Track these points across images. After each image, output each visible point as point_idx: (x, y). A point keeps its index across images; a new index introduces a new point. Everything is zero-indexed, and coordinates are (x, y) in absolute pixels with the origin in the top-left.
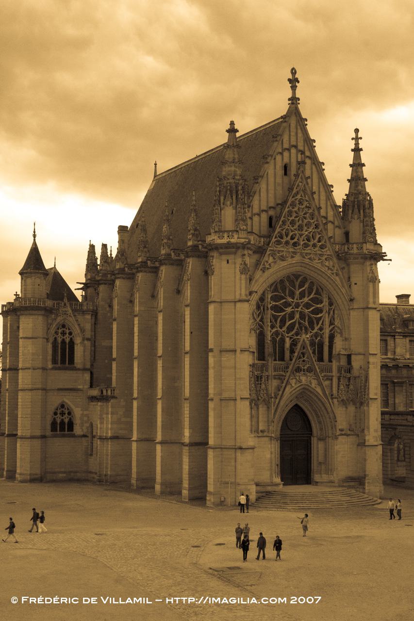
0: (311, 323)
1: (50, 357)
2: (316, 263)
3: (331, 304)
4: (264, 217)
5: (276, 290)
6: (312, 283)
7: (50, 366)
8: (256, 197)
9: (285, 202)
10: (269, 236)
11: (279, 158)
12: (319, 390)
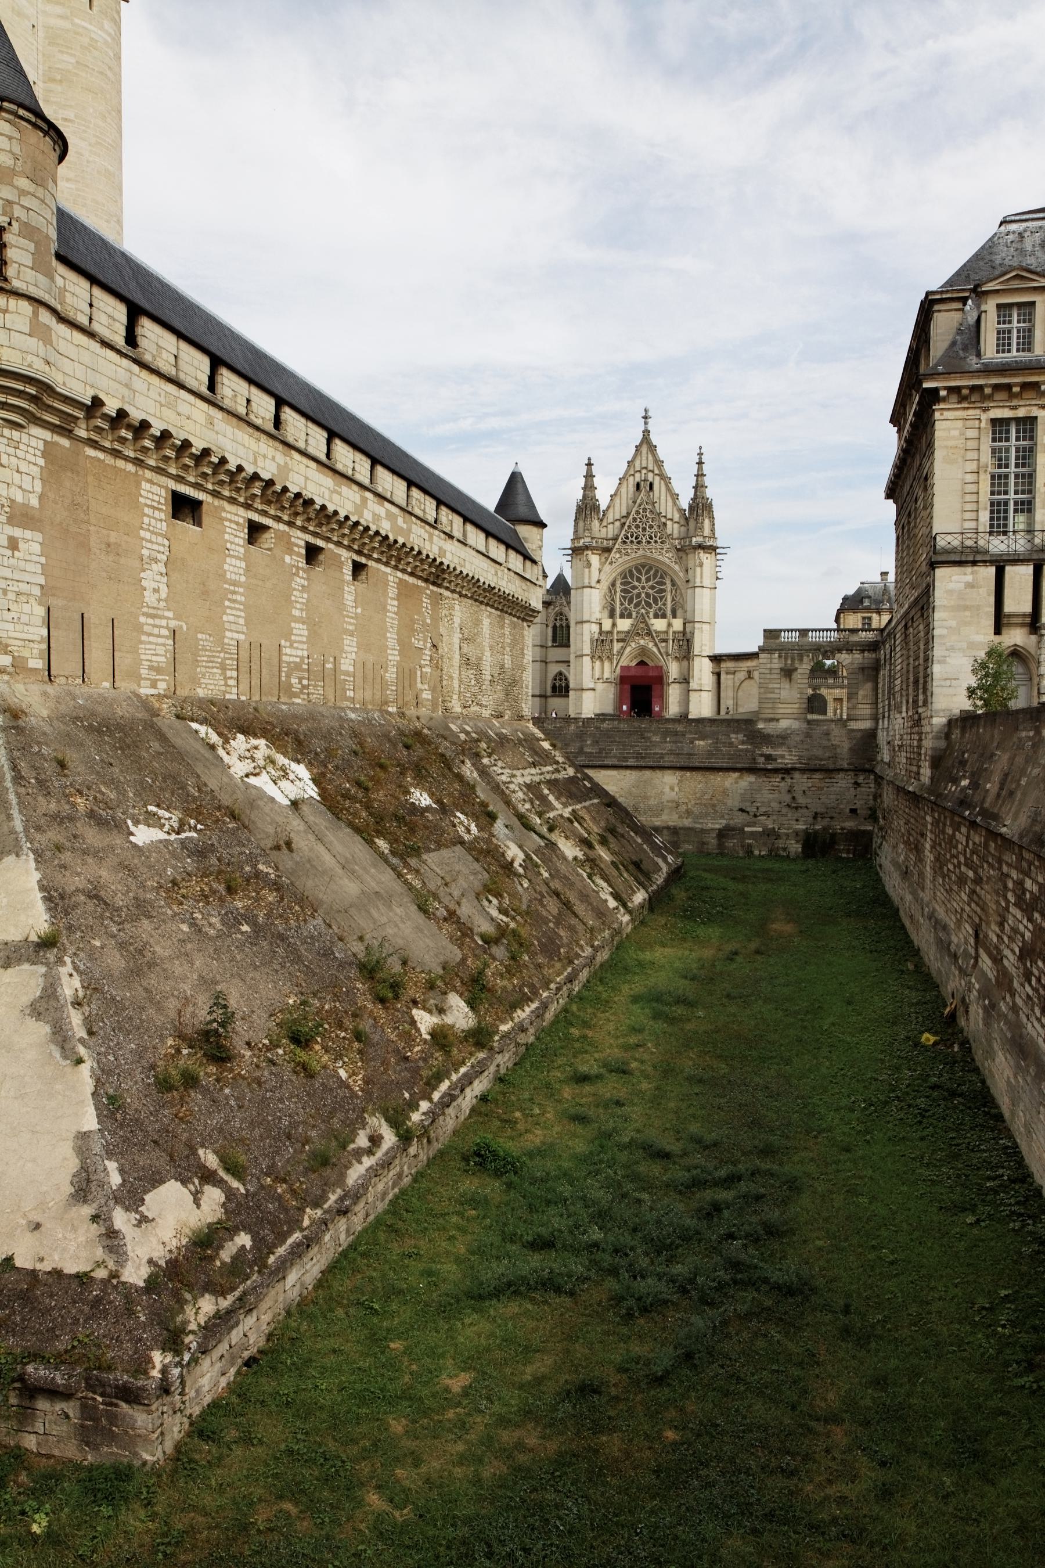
0: (656, 601)
1: (550, 638)
2: (656, 556)
3: (673, 583)
4: (618, 524)
5: (625, 577)
6: (657, 571)
7: (550, 644)
8: (611, 510)
9: (629, 514)
10: (615, 539)
11: (631, 479)
12: (655, 650)
